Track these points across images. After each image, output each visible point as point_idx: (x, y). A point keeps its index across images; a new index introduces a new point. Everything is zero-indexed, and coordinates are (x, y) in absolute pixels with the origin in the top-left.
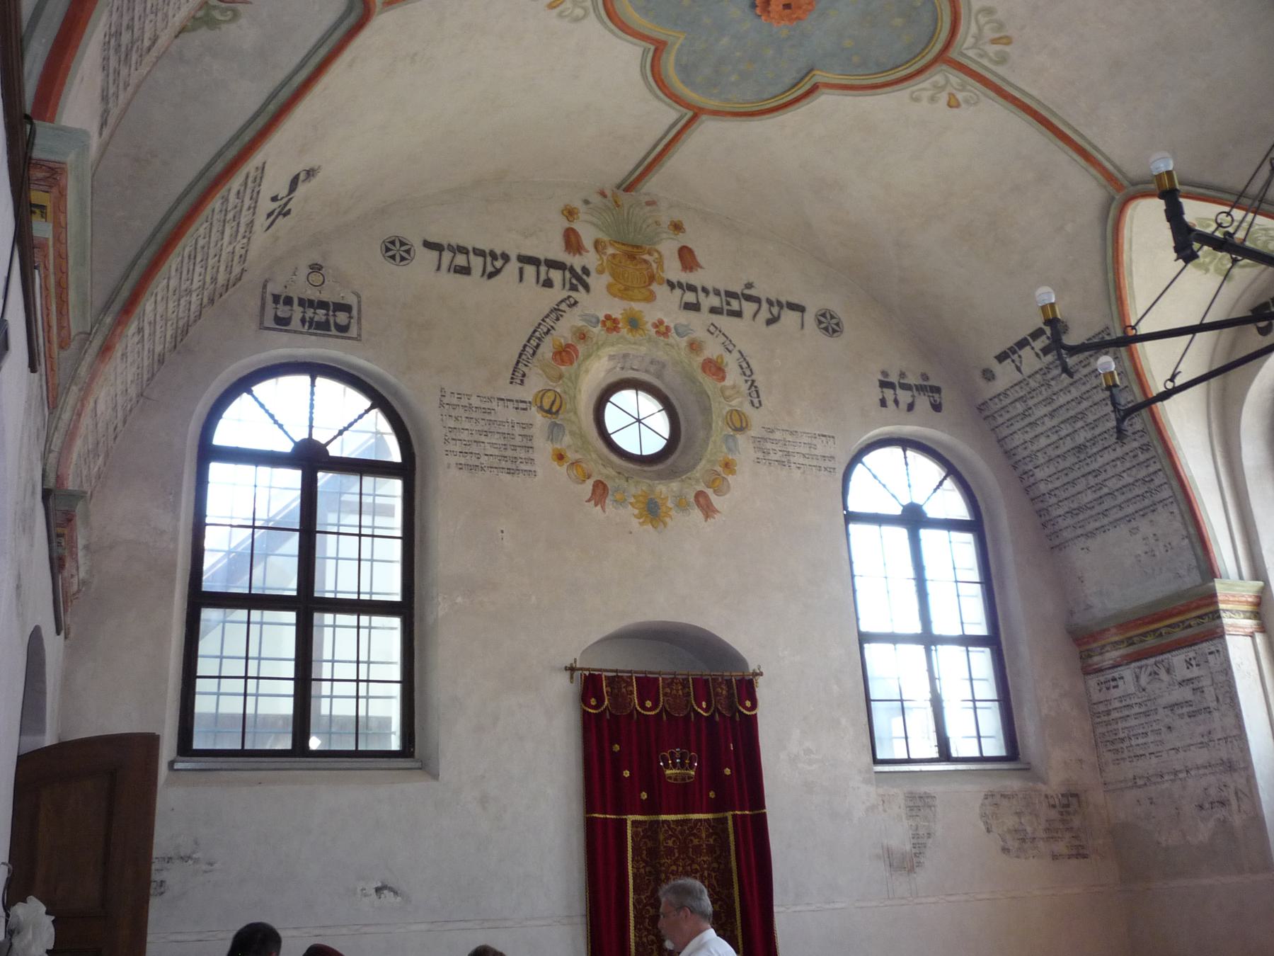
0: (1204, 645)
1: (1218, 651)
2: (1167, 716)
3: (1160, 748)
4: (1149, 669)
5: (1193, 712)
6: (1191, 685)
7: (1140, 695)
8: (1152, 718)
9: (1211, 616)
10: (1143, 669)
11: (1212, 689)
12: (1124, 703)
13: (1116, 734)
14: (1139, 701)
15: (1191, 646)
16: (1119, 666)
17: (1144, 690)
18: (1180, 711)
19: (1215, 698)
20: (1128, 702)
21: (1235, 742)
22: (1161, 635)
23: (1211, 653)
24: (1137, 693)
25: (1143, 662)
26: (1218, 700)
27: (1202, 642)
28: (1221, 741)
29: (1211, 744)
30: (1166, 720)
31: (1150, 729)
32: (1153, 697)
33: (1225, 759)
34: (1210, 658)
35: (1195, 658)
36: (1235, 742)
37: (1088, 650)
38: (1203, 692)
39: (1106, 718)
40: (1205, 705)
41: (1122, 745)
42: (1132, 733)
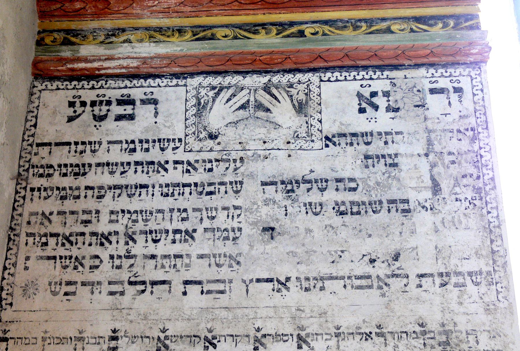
0: (422, 71)
1: (458, 90)
2: (266, 202)
3: (225, 273)
4: (241, 98)
5: (352, 203)
6: (363, 148)
7: (197, 146)
8: (216, 201)
9: (452, 23)
10: (225, 95)
11: (424, 165)
12: (139, 156)
13: (86, 222)
14: (191, 157)
15: (381, 68)
16: (154, 76)
17: (212, 137)
18: (315, 197)
19: (429, 183)
20: (155, 154)
21: (471, 288)
22: (301, 34)
23: (433, 91)
24: (191, 140)
25: (228, 80)
26: (436, 188)
27: (417, 66)
28: (426, 282)
29: (396, 284)
30: (265, 211)
31: (207, 223)
32: (234, 155)
33: (433, 326)
34: (431, 100)
35: (387, 94)
36: (471, 288)
37: (68, 31)
38: (394, 165)
39: (67, 182)
40: (395, 194)
41: (96, 250)
42: (140, 226)
